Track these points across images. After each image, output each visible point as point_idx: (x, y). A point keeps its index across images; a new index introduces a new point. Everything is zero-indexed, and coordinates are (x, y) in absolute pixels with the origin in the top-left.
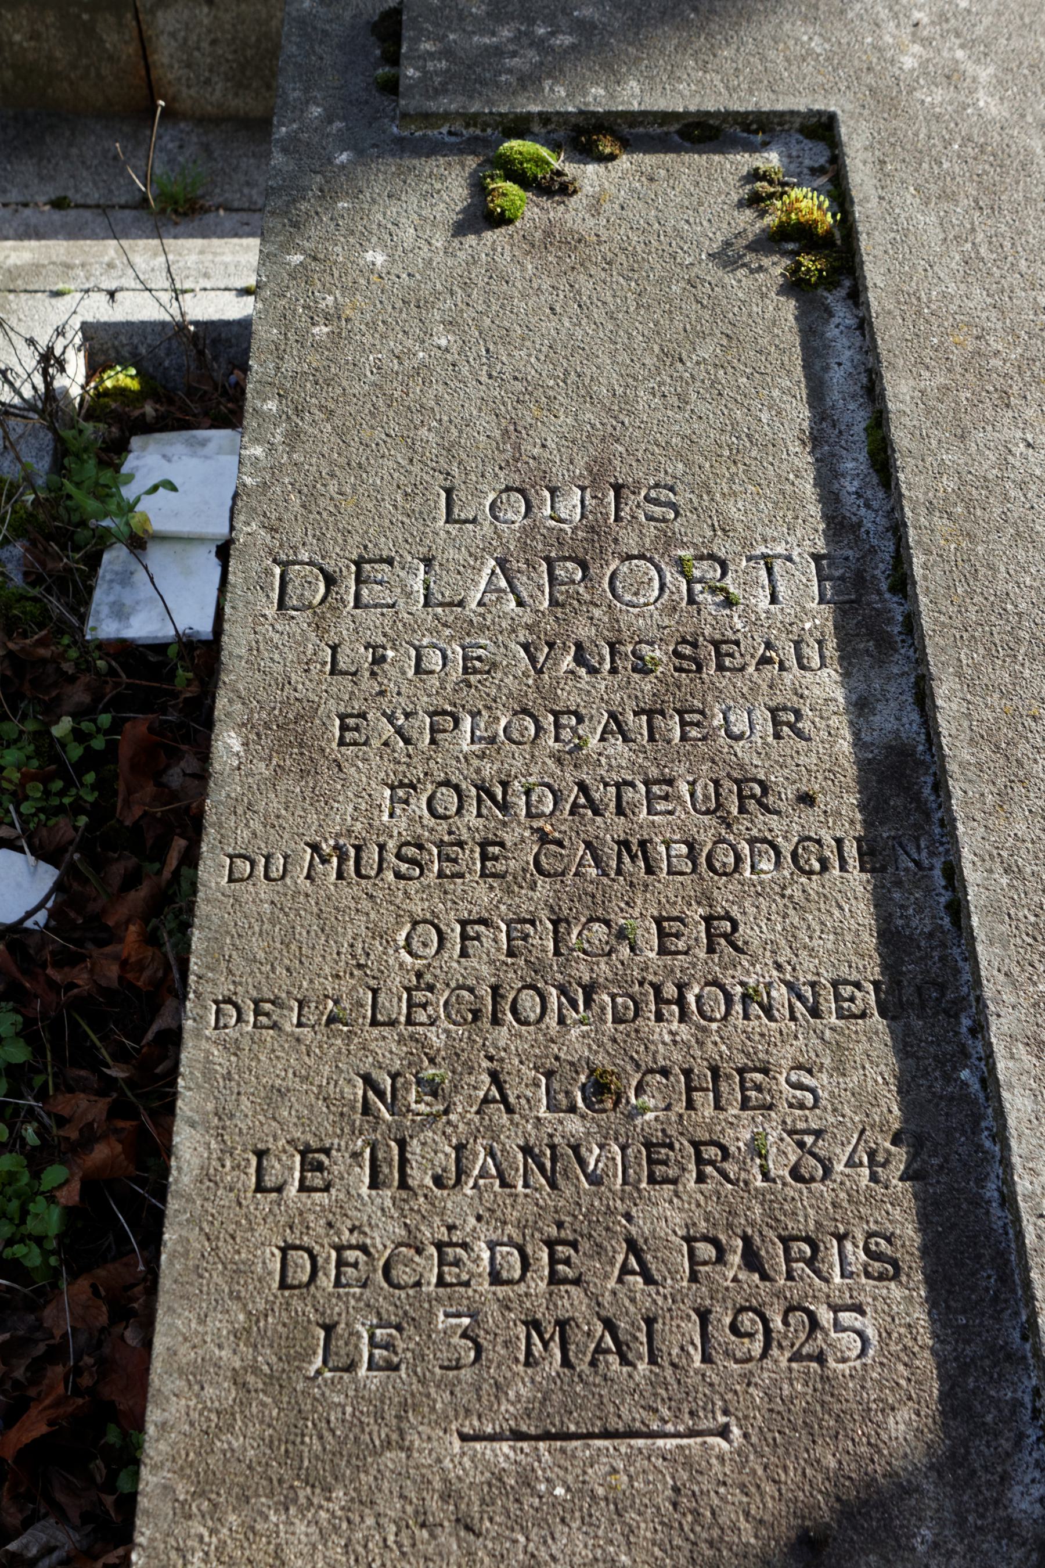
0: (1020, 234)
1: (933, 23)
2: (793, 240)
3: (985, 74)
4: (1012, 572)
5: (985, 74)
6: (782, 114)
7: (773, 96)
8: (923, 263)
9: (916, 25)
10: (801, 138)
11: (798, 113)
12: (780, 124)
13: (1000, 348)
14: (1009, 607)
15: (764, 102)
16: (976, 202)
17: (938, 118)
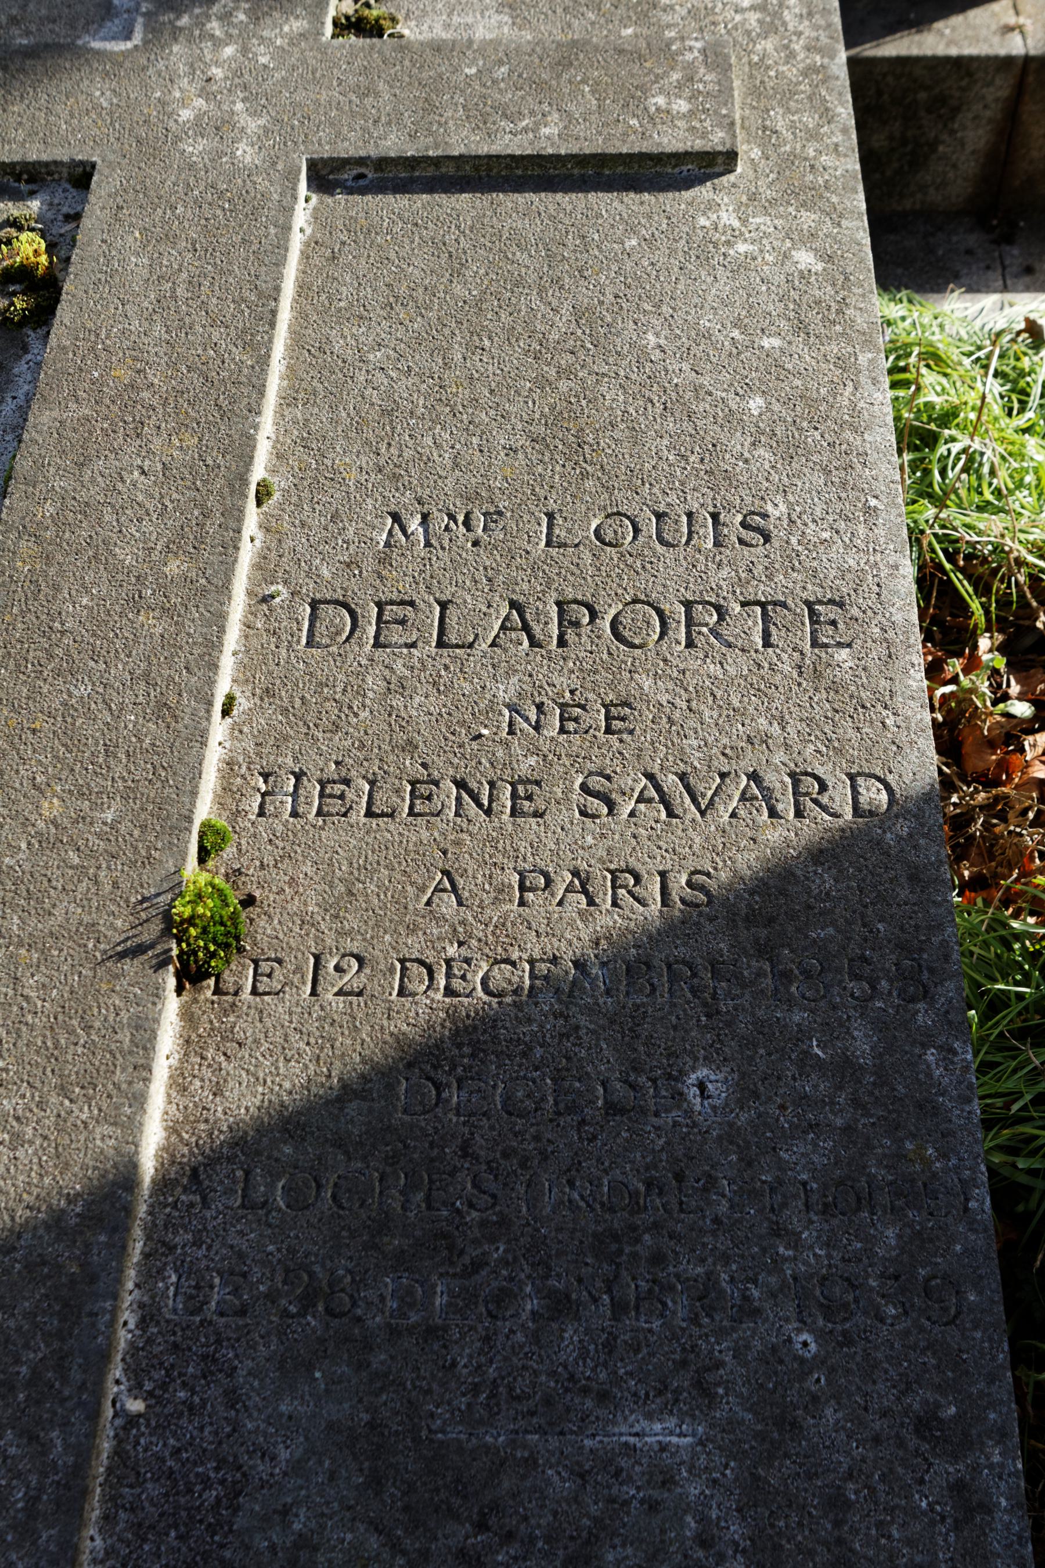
0: (222, 272)
1: (226, 78)
2: (20, 283)
3: (253, 125)
4: (74, 593)
5: (253, 125)
6: (47, 164)
7: (42, 147)
8: (116, 301)
9: (209, 80)
10: (68, 186)
11: (61, 163)
12: (49, 174)
13: (156, 381)
14: (57, 625)
15: (35, 153)
16: (193, 245)
17: (191, 166)
